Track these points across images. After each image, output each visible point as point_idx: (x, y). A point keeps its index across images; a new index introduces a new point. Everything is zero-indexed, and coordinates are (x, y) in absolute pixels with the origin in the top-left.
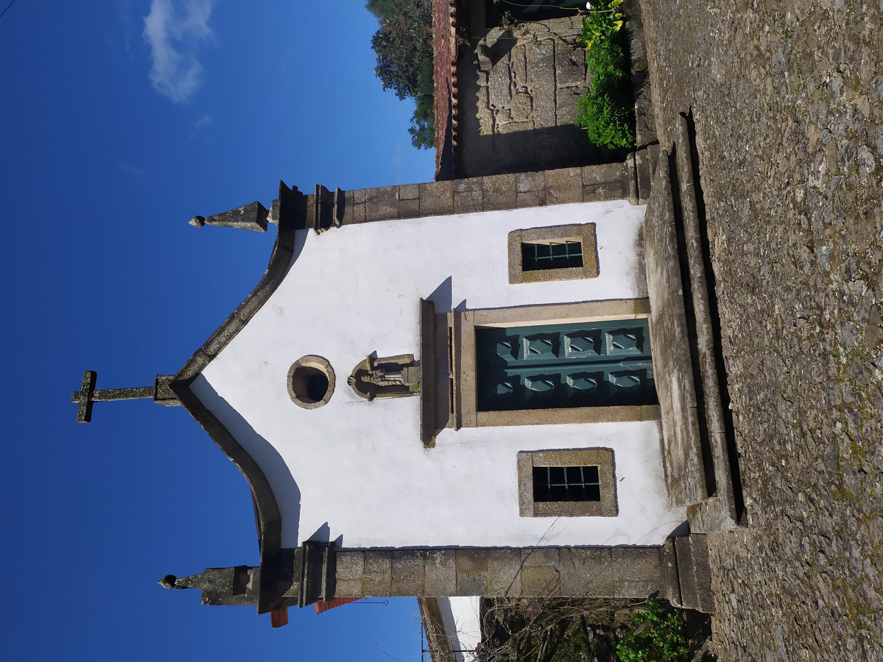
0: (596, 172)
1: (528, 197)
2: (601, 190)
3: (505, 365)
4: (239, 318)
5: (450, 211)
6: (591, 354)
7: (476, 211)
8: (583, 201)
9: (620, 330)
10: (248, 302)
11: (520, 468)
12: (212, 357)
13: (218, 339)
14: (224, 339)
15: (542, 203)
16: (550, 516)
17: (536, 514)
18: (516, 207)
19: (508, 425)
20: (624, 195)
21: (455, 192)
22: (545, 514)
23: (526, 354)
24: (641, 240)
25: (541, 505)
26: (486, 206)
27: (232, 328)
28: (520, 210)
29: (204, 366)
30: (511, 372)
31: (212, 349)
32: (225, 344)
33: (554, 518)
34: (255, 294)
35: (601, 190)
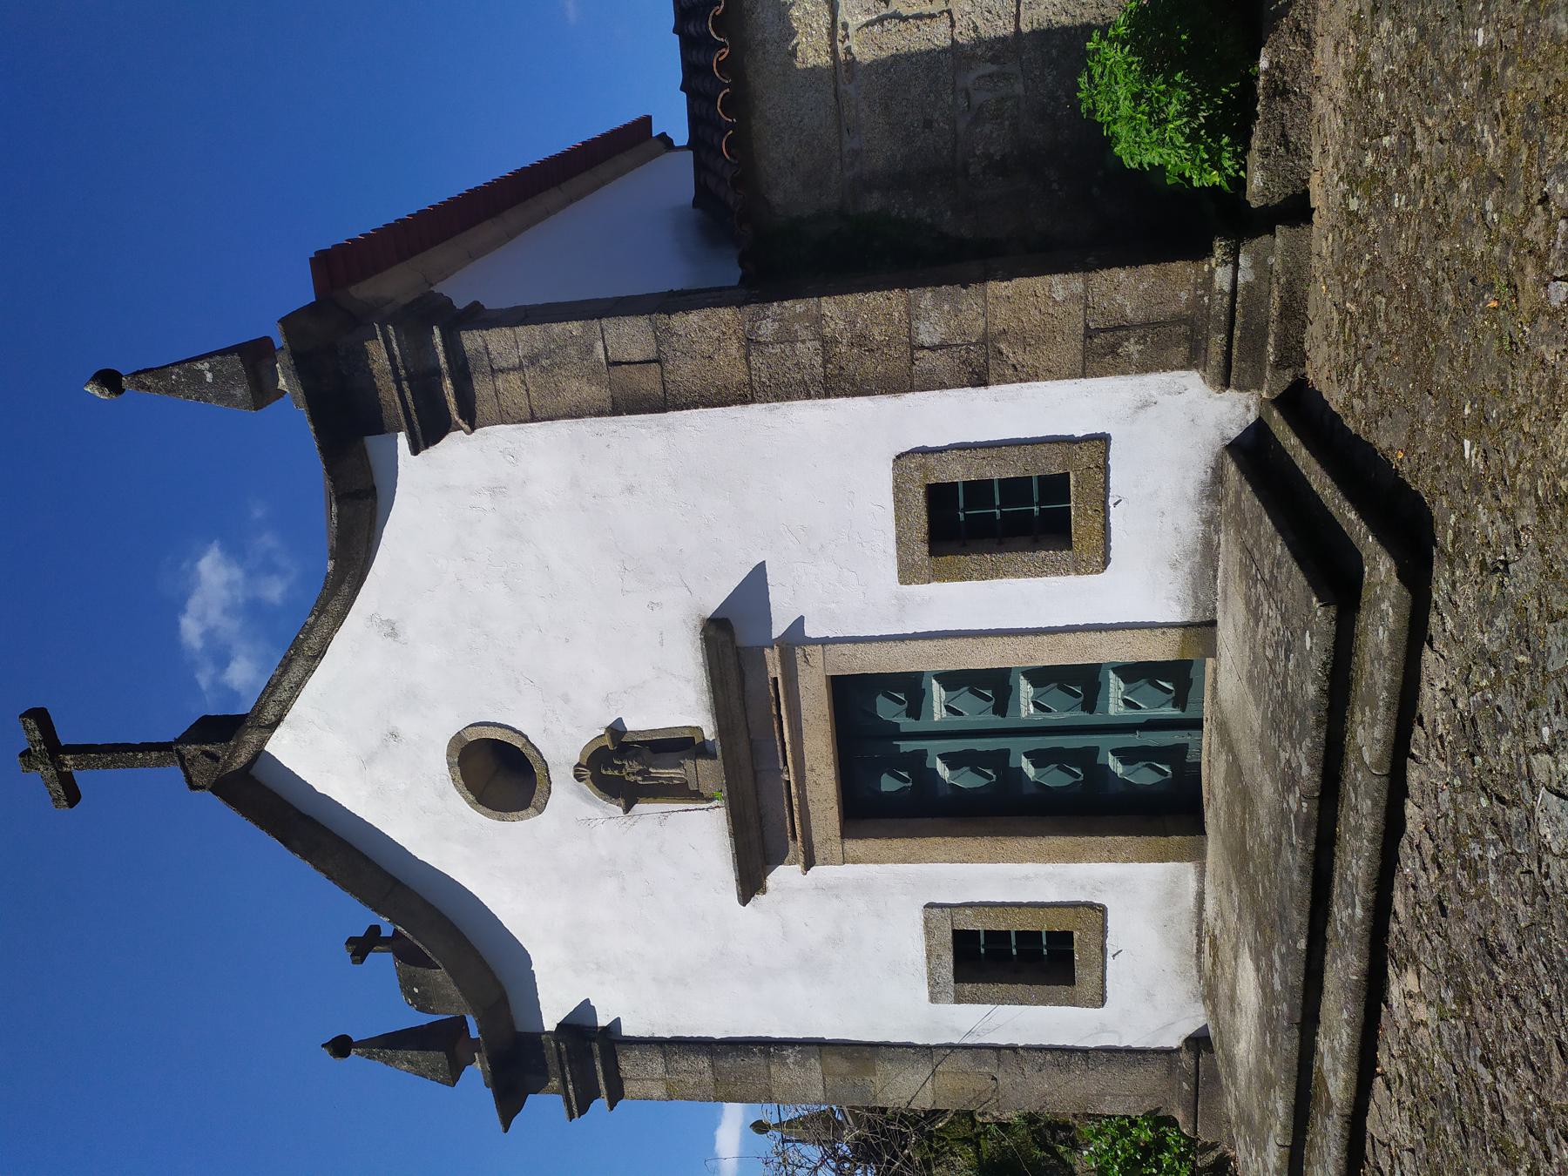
1: (939, 361)
5: (744, 397)
11: (929, 932)
14: (285, 696)
15: (980, 380)
17: (958, 1000)
19: (904, 861)
23: (939, 713)
25: (968, 987)
26: (834, 383)
27: (296, 671)
29: (264, 741)
30: (906, 746)
31: (269, 714)
33: (989, 1007)
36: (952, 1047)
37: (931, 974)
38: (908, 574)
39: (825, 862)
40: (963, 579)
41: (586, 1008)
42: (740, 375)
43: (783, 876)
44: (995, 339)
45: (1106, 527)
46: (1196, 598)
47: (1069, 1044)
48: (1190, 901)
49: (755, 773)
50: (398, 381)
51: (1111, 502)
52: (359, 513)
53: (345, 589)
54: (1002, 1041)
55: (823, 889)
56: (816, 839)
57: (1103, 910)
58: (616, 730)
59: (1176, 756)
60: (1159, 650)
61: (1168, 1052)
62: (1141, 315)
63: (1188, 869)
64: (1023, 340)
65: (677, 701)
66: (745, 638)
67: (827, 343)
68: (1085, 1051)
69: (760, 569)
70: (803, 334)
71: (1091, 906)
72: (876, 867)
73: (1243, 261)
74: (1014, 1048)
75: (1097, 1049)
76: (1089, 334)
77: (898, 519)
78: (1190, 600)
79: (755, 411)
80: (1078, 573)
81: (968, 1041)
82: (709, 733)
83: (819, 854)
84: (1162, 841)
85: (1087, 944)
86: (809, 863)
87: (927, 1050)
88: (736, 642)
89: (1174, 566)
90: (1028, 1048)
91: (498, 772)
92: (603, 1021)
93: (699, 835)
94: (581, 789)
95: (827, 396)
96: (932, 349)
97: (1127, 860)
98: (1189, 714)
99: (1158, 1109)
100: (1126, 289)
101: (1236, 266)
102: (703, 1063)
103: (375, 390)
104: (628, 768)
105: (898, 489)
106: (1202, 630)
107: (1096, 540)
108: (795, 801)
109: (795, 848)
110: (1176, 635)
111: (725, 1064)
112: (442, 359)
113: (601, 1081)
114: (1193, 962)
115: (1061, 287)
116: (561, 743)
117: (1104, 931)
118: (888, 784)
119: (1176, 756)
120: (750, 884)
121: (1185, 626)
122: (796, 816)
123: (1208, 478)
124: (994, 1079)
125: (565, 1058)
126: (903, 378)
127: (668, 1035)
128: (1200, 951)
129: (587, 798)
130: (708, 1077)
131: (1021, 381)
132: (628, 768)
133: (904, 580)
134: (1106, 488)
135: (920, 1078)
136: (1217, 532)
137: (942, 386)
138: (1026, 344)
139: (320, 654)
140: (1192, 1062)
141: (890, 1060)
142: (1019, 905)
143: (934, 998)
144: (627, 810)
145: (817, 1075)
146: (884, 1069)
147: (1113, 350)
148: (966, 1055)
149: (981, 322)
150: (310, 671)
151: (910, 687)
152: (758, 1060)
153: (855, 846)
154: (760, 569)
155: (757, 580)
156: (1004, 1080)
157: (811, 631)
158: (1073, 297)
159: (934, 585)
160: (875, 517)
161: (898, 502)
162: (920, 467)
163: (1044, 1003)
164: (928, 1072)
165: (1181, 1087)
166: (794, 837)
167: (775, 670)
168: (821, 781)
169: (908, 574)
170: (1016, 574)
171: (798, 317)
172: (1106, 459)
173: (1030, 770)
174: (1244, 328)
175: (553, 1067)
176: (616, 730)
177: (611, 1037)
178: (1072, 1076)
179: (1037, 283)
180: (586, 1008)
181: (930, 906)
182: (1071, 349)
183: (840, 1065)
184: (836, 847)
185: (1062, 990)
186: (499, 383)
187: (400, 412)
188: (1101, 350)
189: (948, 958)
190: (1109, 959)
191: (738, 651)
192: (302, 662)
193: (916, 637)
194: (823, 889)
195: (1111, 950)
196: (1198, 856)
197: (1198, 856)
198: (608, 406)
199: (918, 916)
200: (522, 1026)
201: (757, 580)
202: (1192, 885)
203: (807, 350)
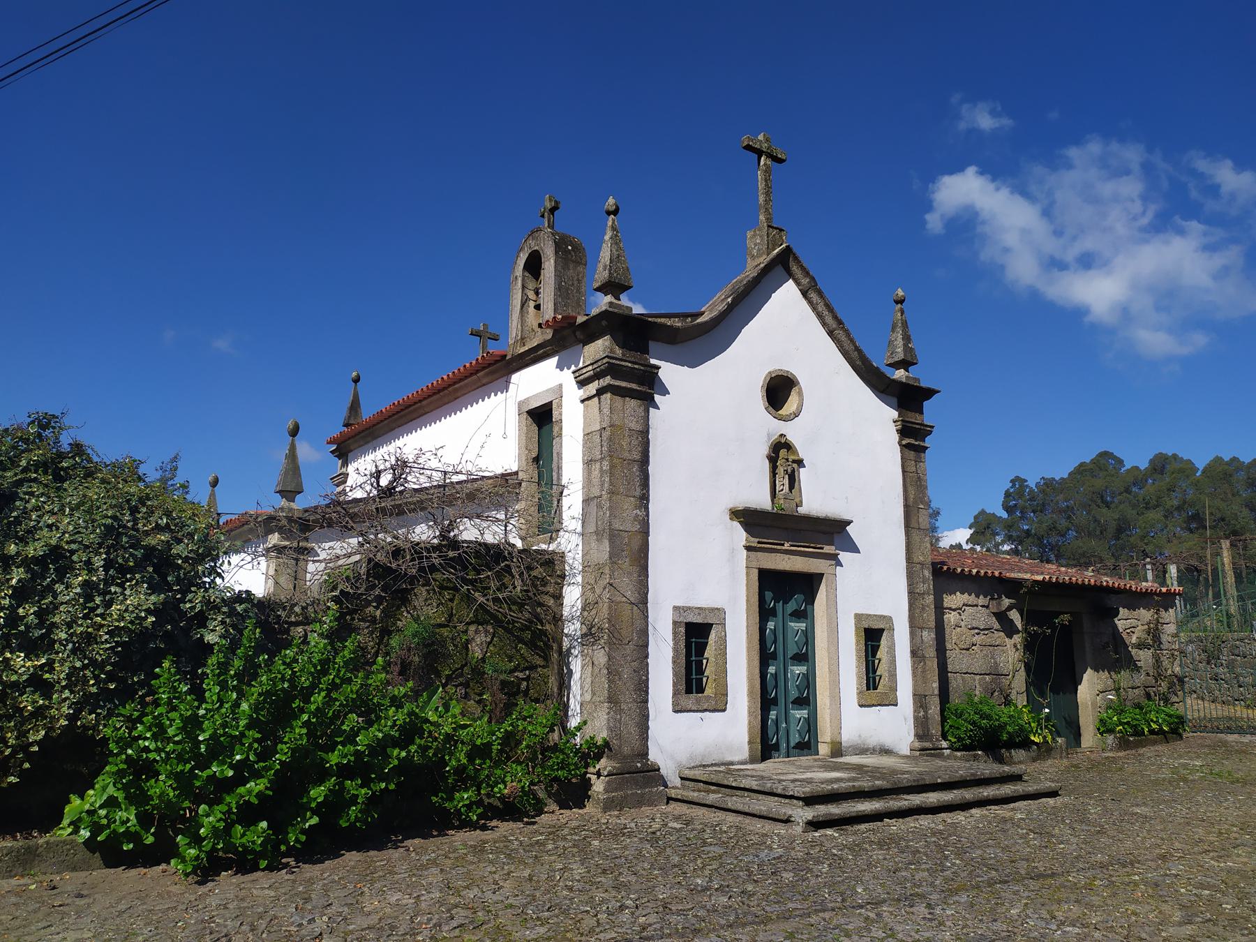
0: (934, 710)
3: (786, 602)
4: (836, 328)
5: (909, 559)
6: (794, 694)
7: (909, 585)
8: (914, 695)
9: (811, 725)
11: (713, 610)
12: (805, 294)
17: (675, 623)
19: (747, 601)
21: (922, 564)
22: (675, 633)
24: (886, 751)
25: (683, 630)
26: (912, 594)
27: (829, 319)
31: (813, 296)
32: (814, 309)
33: (671, 643)
34: (857, 349)
37: (690, 608)
38: (858, 617)
39: (748, 557)
41: (665, 392)
42: (916, 560)
43: (740, 535)
48: (729, 758)
56: (759, 554)
57: (724, 710)
58: (800, 463)
59: (776, 747)
60: (825, 734)
61: (647, 754)
63: (744, 753)
64: (924, 672)
65: (816, 499)
68: (647, 701)
81: (650, 628)
83: (752, 554)
87: (645, 601)
88: (831, 533)
91: (779, 390)
92: (657, 398)
97: (750, 722)
99: (610, 750)
102: (636, 455)
106: (837, 750)
109: (754, 542)
114: (698, 763)
116: (795, 432)
126: (915, 625)
130: (626, 455)
139: (831, 333)
143: (676, 608)
150: (824, 324)
151: (804, 614)
152: (638, 493)
153: (755, 573)
155: (855, 550)
161: (881, 616)
167: (828, 549)
169: (858, 617)
177: (648, 401)
180: (665, 392)
182: (921, 692)
184: (755, 564)
185: (683, 687)
188: (920, 700)
196: (752, 760)
197: (752, 760)
200: (652, 345)
201: (855, 550)
202: (736, 758)
203: (921, 588)
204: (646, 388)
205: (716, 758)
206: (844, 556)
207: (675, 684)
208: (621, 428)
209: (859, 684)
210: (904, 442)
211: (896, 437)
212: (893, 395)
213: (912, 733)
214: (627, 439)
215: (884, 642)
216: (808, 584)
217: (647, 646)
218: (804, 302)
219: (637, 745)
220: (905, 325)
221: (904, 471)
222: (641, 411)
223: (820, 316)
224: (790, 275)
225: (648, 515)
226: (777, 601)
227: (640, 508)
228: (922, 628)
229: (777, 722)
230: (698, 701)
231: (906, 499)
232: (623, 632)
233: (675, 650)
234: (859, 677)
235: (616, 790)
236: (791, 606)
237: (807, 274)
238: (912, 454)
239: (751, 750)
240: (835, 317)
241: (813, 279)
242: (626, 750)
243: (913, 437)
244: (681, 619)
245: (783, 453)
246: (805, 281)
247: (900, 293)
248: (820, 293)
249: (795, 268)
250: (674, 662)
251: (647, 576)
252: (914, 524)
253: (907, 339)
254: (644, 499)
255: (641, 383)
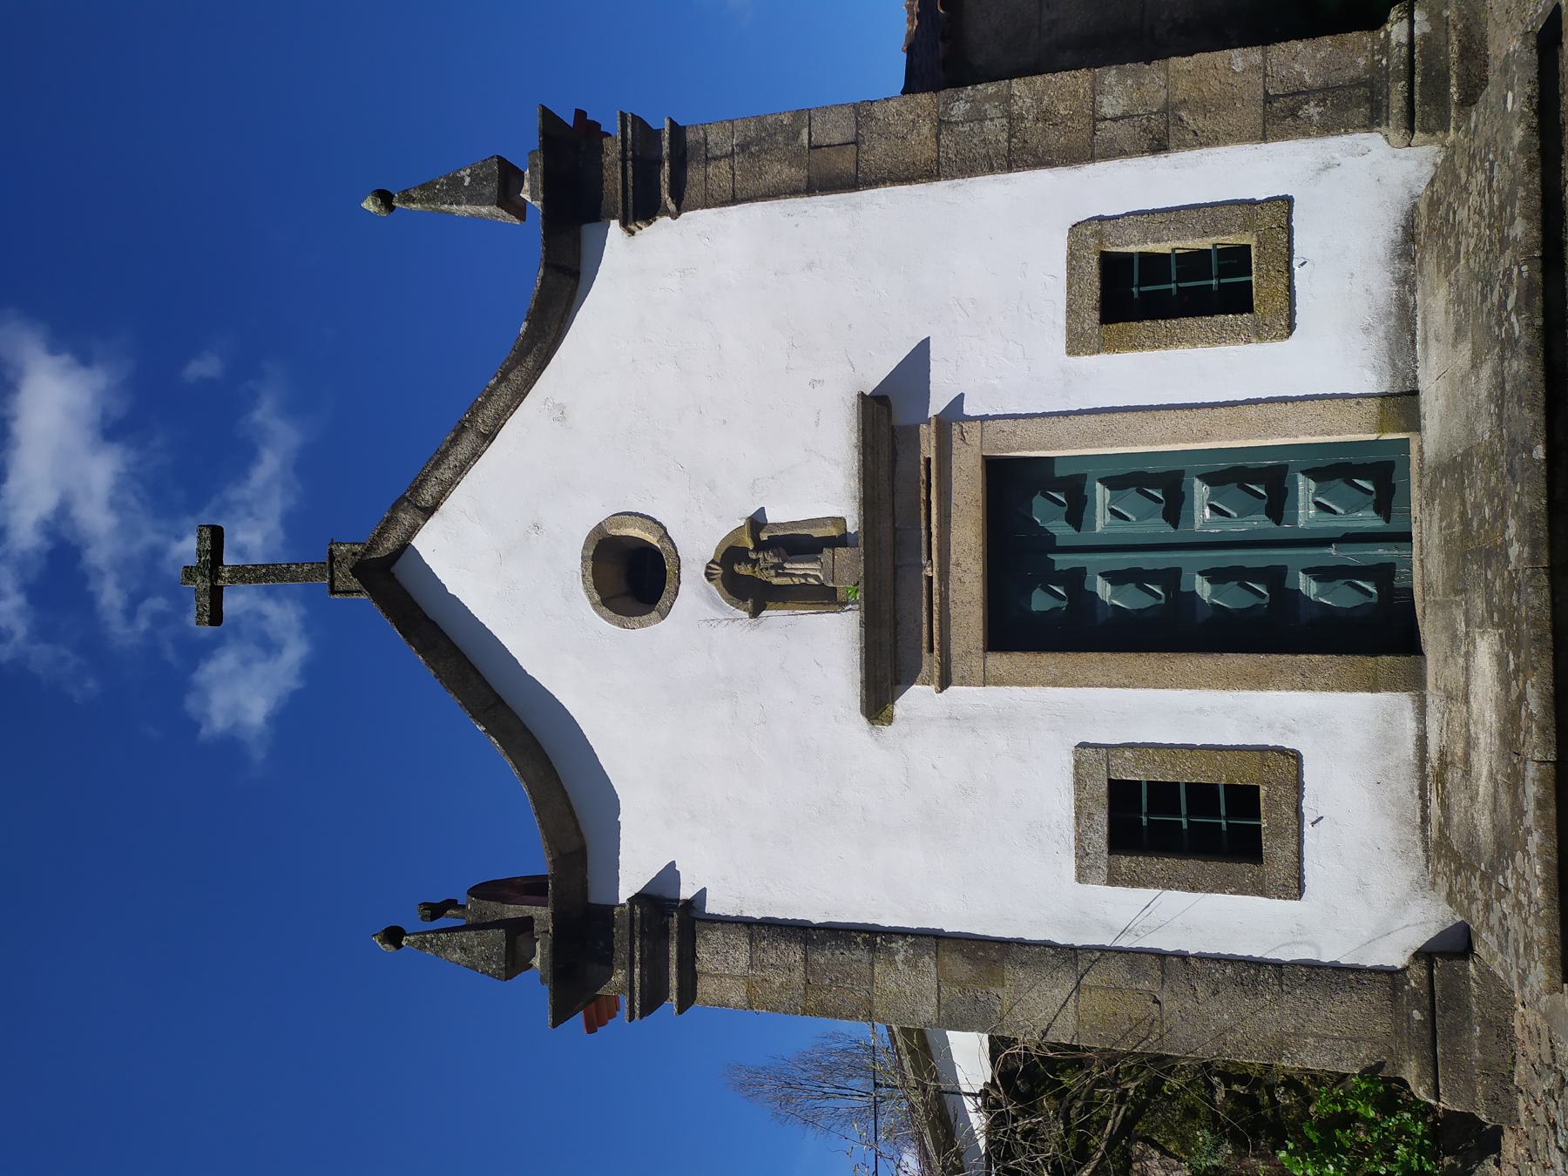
1: (1122, 131)
2: (1312, 110)
3: (1049, 543)
4: (471, 426)
5: (930, 173)
7: (992, 170)
8: (1264, 139)
10: (490, 394)
11: (1079, 781)
12: (429, 511)
13: (437, 473)
14: (448, 475)
15: (1159, 146)
16: (1145, 886)
17: (1112, 880)
18: (1092, 159)
19: (1055, 683)
20: (1373, 121)
22: (1134, 882)
23: (1101, 521)
25: (1125, 861)
27: (463, 450)
28: (1100, 166)
29: (414, 530)
30: (1062, 561)
31: (427, 495)
32: (453, 483)
33: (1151, 893)
34: (504, 378)
35: (1312, 110)
36: (1103, 950)
37: (1079, 839)
38: (1077, 344)
39: (964, 682)
40: (1134, 348)
41: (670, 874)
42: (929, 152)
43: (917, 699)
44: (1175, 107)
45: (1290, 288)
46: (1394, 365)
47: (1257, 954)
48: (1409, 749)
49: (896, 568)
50: (624, 160)
51: (1295, 264)
52: (564, 282)
53: (530, 362)
54: (1168, 946)
55: (955, 719)
56: (955, 650)
57: (1296, 757)
58: (756, 522)
59: (1383, 573)
60: (1355, 430)
61: (1391, 972)
62: (1320, 81)
63: (1400, 702)
64: (1203, 107)
66: (900, 419)
67: (1013, 120)
68: (1278, 965)
69: (925, 344)
70: (992, 112)
71: (1282, 751)
72: (1017, 691)
73: (1419, 16)
74: (1183, 957)
75: (1293, 964)
76: (1268, 99)
77: (1070, 286)
78: (1387, 368)
79: (941, 187)
80: (1261, 339)
81: (1125, 943)
82: (853, 526)
83: (957, 670)
84: (1369, 662)
85: (1278, 805)
86: (945, 683)
87: (1070, 955)
88: (892, 423)
89: (1366, 330)
90: (1201, 957)
92: (686, 892)
93: (829, 642)
94: (709, 591)
95: (1009, 169)
96: (1115, 119)
97: (1327, 688)
98: (1395, 526)
99: (1381, 1065)
100: (1302, 60)
101: (1412, 22)
102: (795, 954)
103: (600, 180)
104: (762, 569)
105: (1072, 256)
106: (1402, 404)
107: (1280, 302)
108: (936, 599)
109: (930, 663)
110: (1373, 406)
111: (819, 958)
112: (666, 144)
113: (673, 969)
114: (1417, 837)
115: (1240, 59)
116: (696, 541)
117: (1299, 787)
118: (1040, 602)
119: (1383, 573)
120: (877, 702)
121: (1383, 396)
122: (935, 616)
123: (1399, 236)
124: (1156, 1001)
125: (637, 928)
126: (1085, 147)
127: (757, 915)
128: (1425, 819)
129: (715, 603)
130: (798, 976)
131: (1201, 145)
132: (762, 569)
133: (1072, 350)
134: (1290, 249)
135: (1060, 994)
136: (1413, 291)
137: (1123, 153)
138: (1205, 112)
139: (489, 437)
140: (1423, 973)
141: (1023, 964)
142: (1192, 747)
143: (1081, 877)
144: (755, 613)
145: (930, 982)
146: (1016, 975)
147: (1293, 113)
148: (1120, 961)
149: (1163, 93)
150: (476, 455)
151: (1072, 487)
152: (861, 954)
153: (1001, 662)
154: (923, 348)
155: (920, 357)
156: (1171, 1005)
157: (968, 410)
158: (1252, 68)
159: (1103, 358)
160: (1046, 284)
161: (1071, 270)
162: (1096, 234)
163: (1221, 888)
164: (1070, 985)
165: (1409, 1017)
166: (931, 650)
167: (928, 449)
168: (967, 579)
169: (1077, 344)
170: (1193, 342)
171: (989, 98)
172: (1289, 220)
173: (1203, 588)
174: (1425, 74)
175: (621, 955)
176: (756, 522)
177: (693, 915)
178: (1261, 1001)
179: (1219, 57)
180: (670, 874)
181: (1083, 745)
182: (1252, 115)
183: (961, 968)
184: (976, 663)
185: (1245, 870)
186: (710, 170)
187: (620, 198)
188: (1279, 116)
189: (1101, 818)
190: (1307, 828)
191: (893, 429)
192: (472, 436)
193: (1080, 412)
194: (955, 719)
195: (1309, 817)
196: (1415, 683)
197: (1415, 683)
198: (803, 185)
199: (1068, 761)
200: (596, 897)
202: (1410, 727)
203: (995, 127)
204: (670, 915)
205: (1405, 786)
206: (937, 406)
207: (1242, 891)
208: (750, 987)
209: (1236, 336)
210: (672, 207)
211: (663, 222)
212: (577, 240)
213: (1361, 139)
214: (769, 973)
215: (1134, 245)
216: (1010, 482)
217: (1161, 955)
218: (446, 506)
219: (1377, 995)
220: (429, 191)
221: (734, 200)
222: (715, 936)
223: (462, 469)
224: (405, 547)
225: (903, 933)
226: (1050, 576)
227: (891, 953)
228: (1097, 119)
229: (1322, 574)
230: (1278, 832)
231: (794, 192)
232: (1137, 1013)
233: (1168, 884)
234: (1219, 339)
235: (1470, 1083)
236: (1061, 530)
237: (390, 521)
238: (694, 174)
239: (1392, 687)
240: (455, 441)
241: (395, 507)
242: (1382, 1026)
243: (658, 176)
244: (1103, 864)
245: (743, 570)
246: (406, 518)
247: (369, 205)
248: (417, 487)
249: (389, 544)
250: (1193, 889)
251: (1021, 943)
252: (844, 162)
253: (454, 191)
254: (873, 938)
255: (665, 932)
